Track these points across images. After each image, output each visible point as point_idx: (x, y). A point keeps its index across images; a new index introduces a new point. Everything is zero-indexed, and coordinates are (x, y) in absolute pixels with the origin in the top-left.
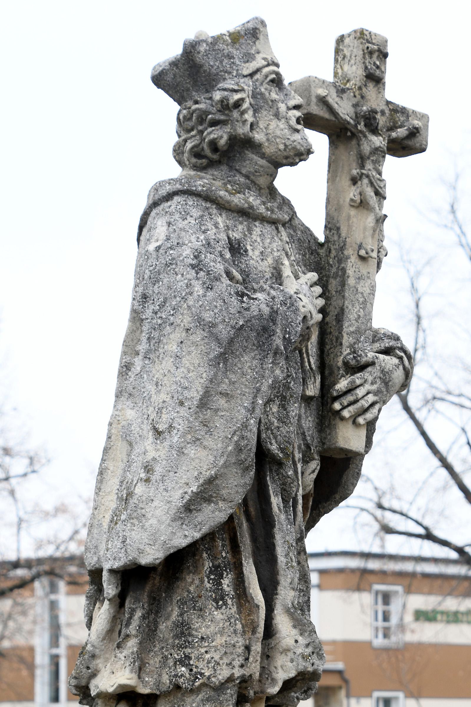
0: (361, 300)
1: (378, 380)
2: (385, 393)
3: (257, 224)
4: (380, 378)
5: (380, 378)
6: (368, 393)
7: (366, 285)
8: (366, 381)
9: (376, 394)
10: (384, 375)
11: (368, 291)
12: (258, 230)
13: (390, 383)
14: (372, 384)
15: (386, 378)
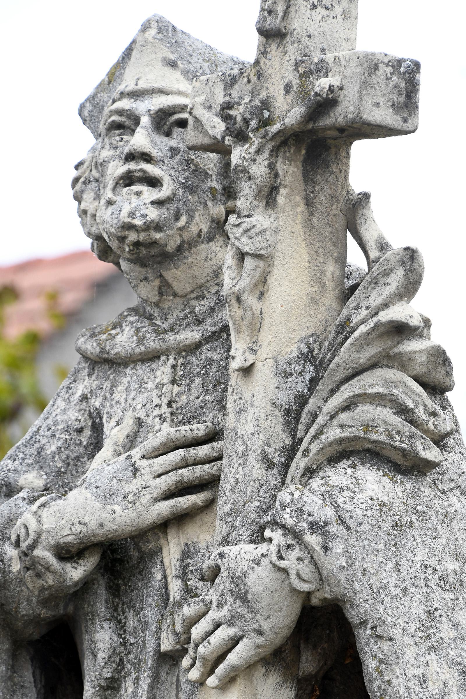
0: (241, 449)
1: (228, 597)
2: (249, 616)
3: (128, 371)
4: (231, 591)
5: (231, 591)
6: (218, 626)
7: (249, 420)
8: (208, 607)
9: (231, 623)
10: (237, 585)
11: (252, 429)
12: (125, 381)
13: (250, 596)
14: (220, 605)
15: (240, 589)
